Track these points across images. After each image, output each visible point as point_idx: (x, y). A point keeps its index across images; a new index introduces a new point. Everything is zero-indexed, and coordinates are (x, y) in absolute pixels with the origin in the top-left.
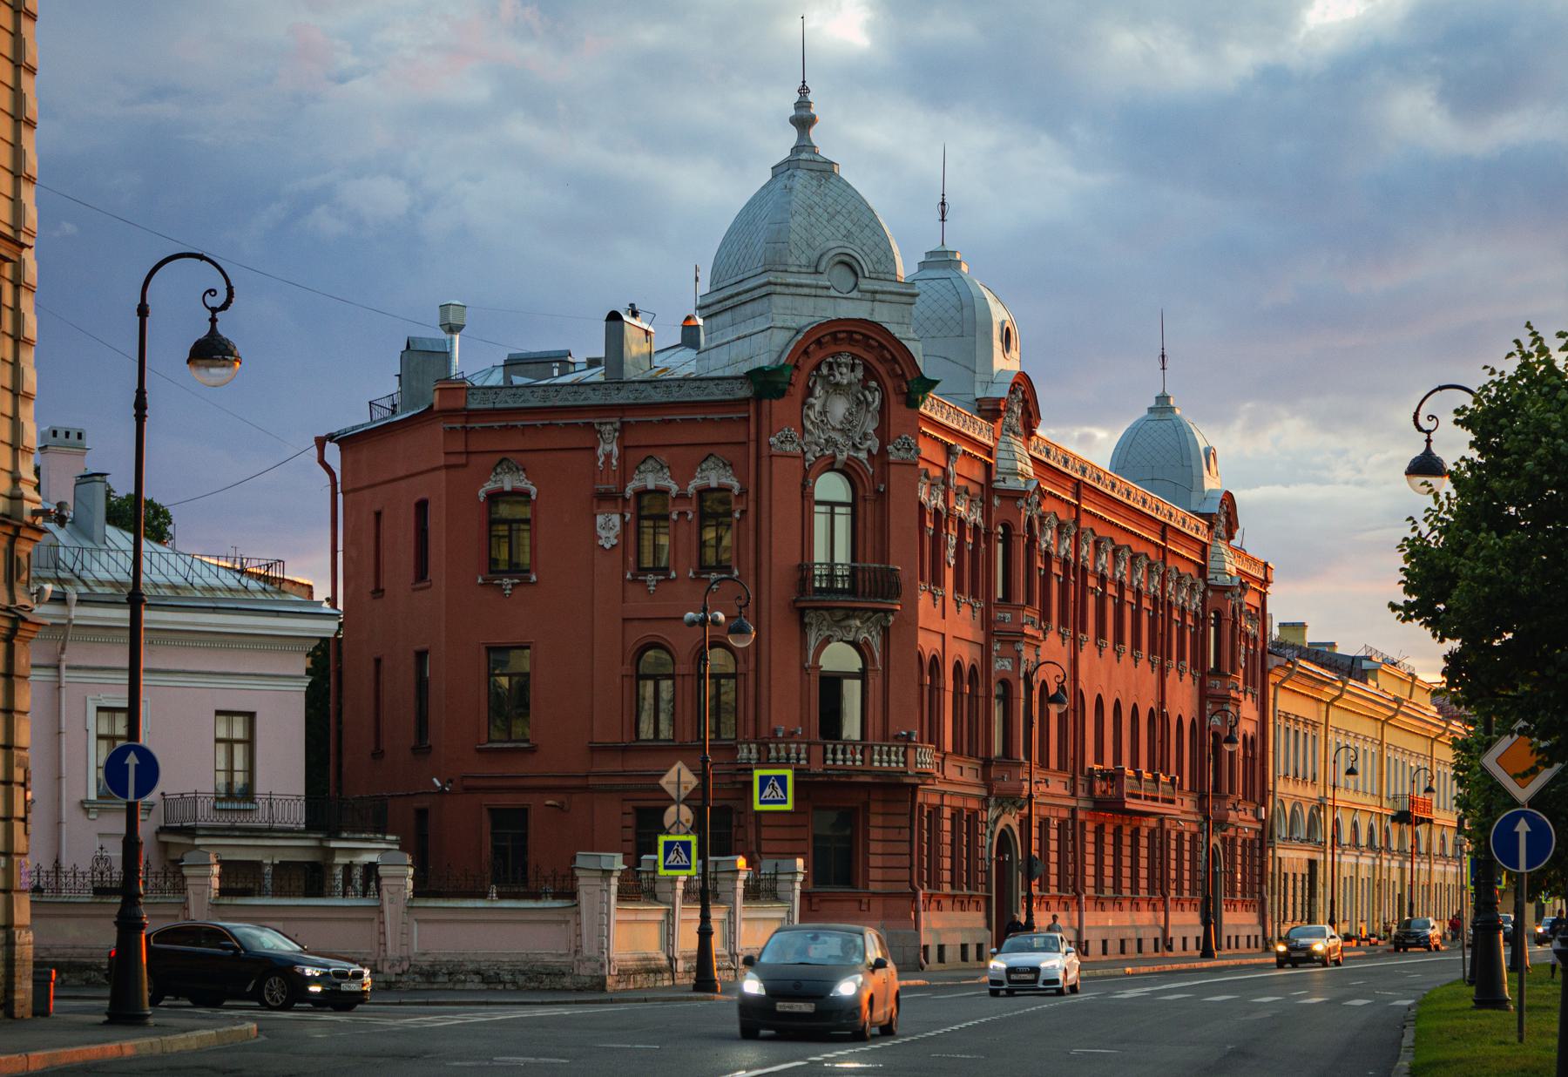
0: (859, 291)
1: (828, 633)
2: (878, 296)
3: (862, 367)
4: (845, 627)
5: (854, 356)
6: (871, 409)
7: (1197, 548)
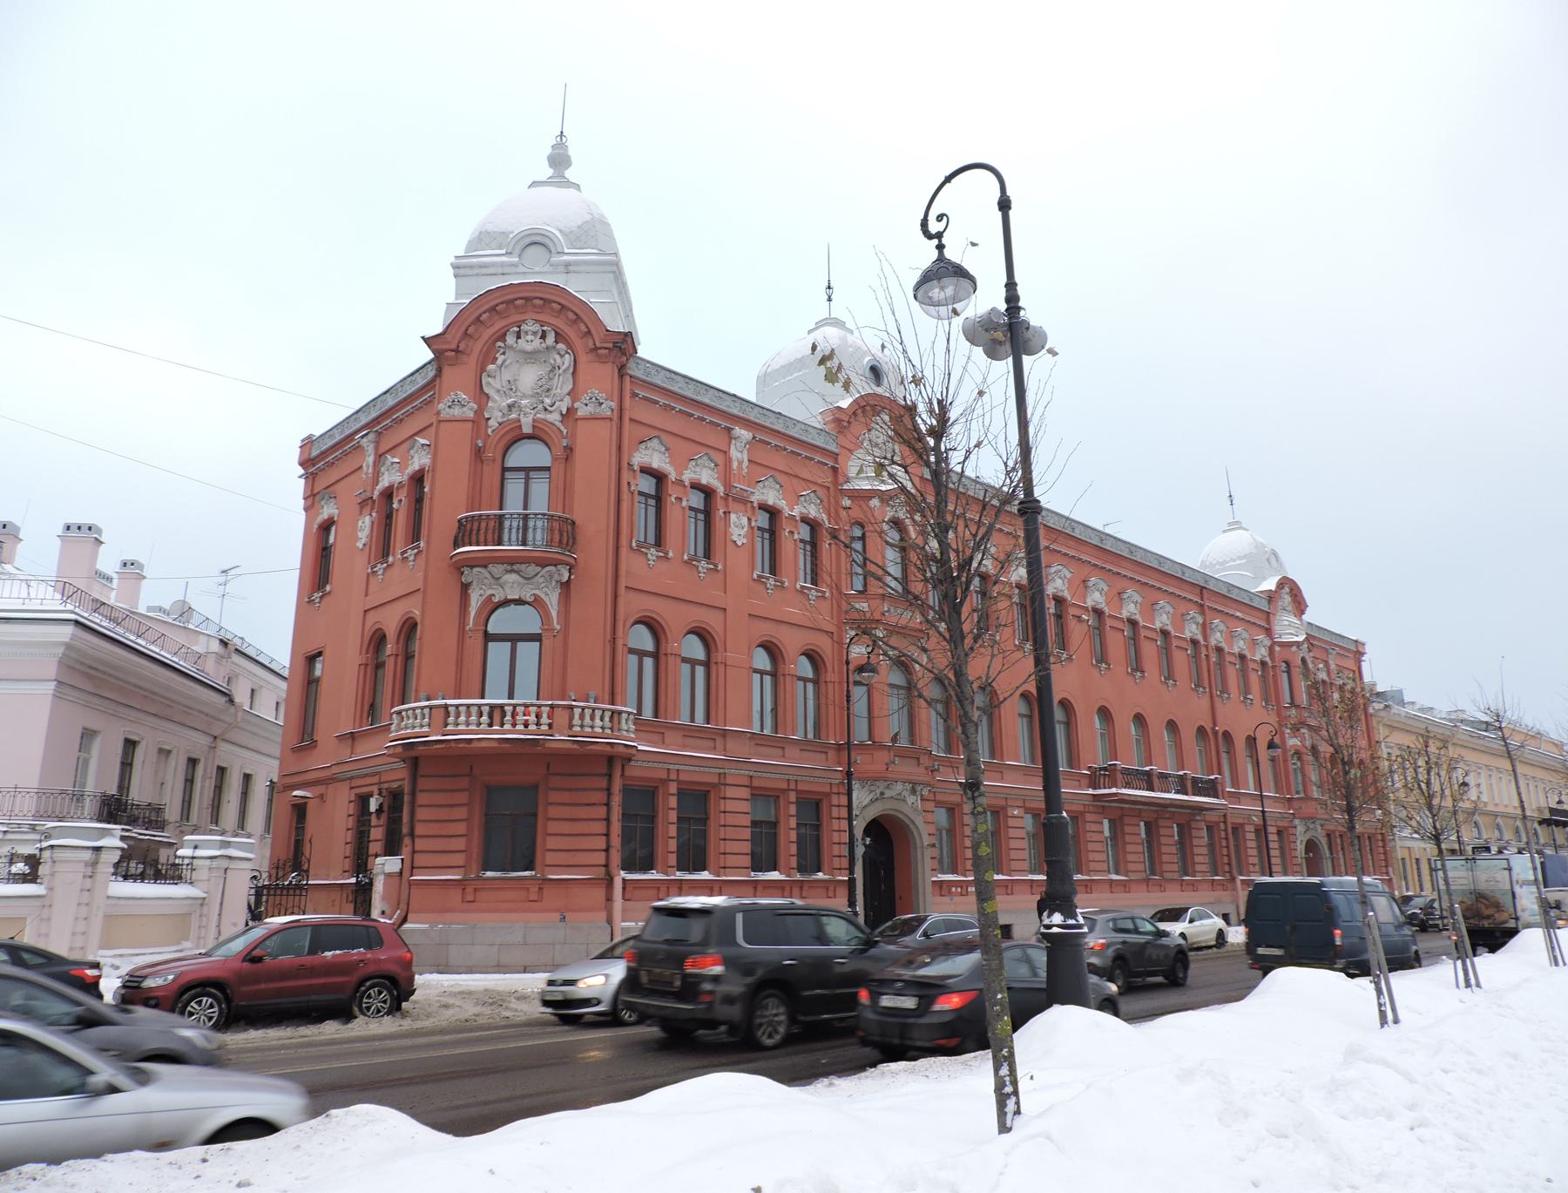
0: (551, 265)
3: (553, 333)
7: (1264, 617)
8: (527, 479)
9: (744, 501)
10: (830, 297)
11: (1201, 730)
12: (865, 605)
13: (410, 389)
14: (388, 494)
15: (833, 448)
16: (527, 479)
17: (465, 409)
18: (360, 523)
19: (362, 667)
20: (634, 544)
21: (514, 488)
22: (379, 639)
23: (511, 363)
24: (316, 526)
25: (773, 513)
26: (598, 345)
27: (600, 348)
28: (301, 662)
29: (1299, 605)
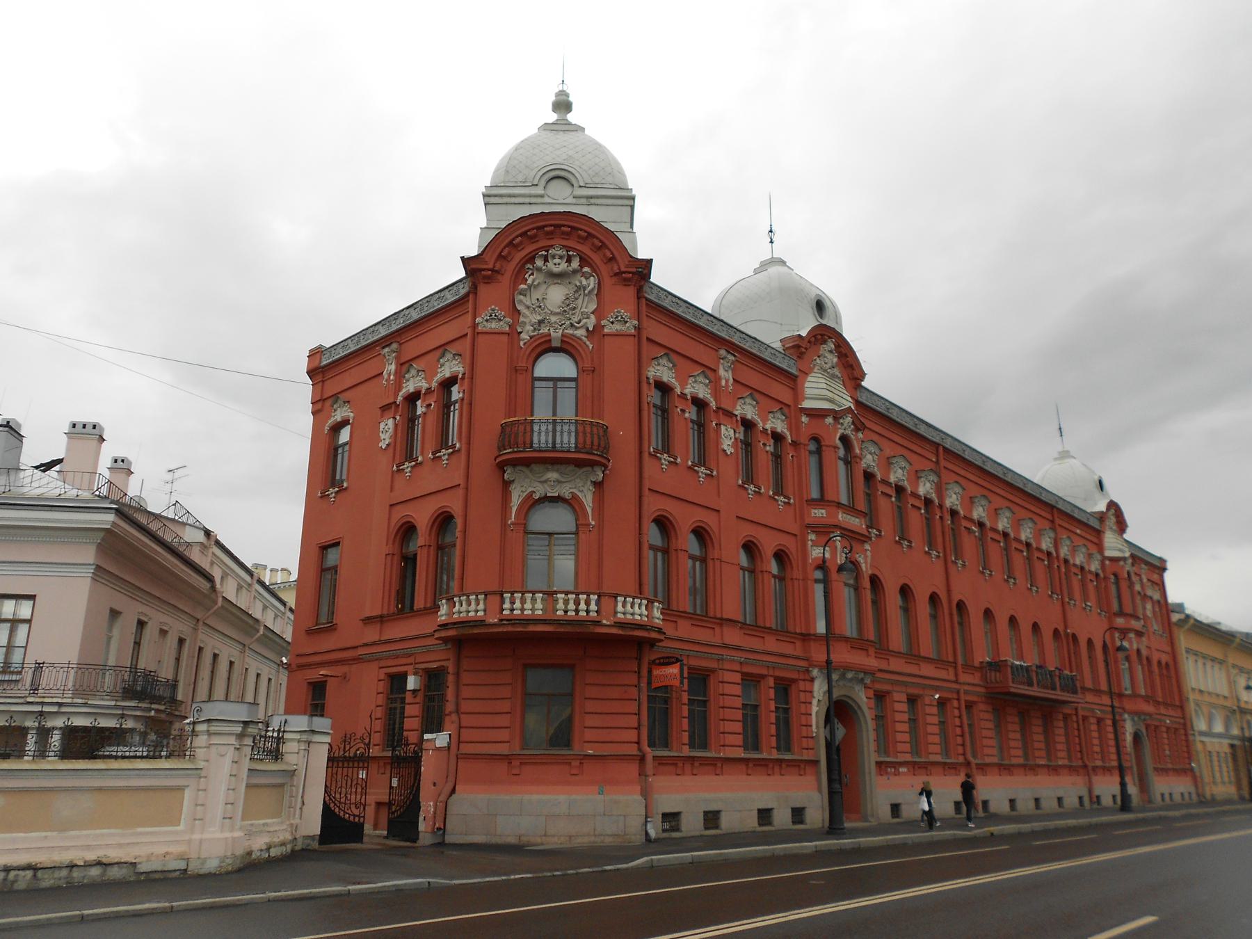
1: (530, 489)
2: (592, 201)
4: (545, 482)
5: (568, 249)
6: (586, 292)
8: (555, 388)
9: (730, 414)
10: (771, 239)
11: (1056, 631)
12: (823, 511)
13: (438, 305)
14: (413, 398)
15: (794, 371)
16: (555, 388)
17: (501, 323)
18: (382, 425)
19: (389, 558)
20: (652, 450)
21: (542, 396)
22: (408, 530)
23: (539, 284)
24: (327, 428)
25: (748, 425)
26: (623, 269)
27: (624, 273)
28: (315, 552)
29: (1121, 526)
